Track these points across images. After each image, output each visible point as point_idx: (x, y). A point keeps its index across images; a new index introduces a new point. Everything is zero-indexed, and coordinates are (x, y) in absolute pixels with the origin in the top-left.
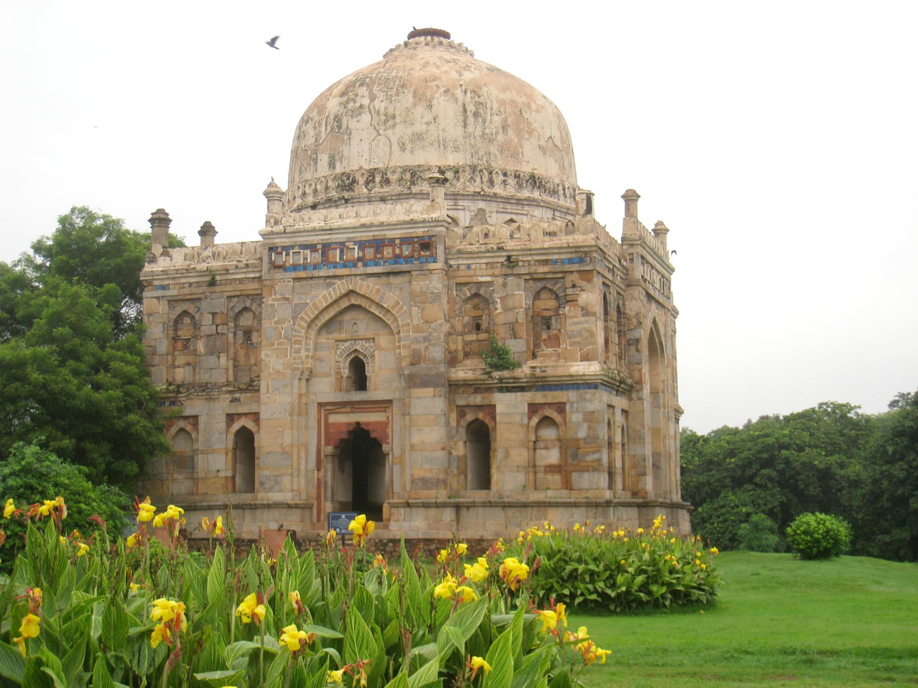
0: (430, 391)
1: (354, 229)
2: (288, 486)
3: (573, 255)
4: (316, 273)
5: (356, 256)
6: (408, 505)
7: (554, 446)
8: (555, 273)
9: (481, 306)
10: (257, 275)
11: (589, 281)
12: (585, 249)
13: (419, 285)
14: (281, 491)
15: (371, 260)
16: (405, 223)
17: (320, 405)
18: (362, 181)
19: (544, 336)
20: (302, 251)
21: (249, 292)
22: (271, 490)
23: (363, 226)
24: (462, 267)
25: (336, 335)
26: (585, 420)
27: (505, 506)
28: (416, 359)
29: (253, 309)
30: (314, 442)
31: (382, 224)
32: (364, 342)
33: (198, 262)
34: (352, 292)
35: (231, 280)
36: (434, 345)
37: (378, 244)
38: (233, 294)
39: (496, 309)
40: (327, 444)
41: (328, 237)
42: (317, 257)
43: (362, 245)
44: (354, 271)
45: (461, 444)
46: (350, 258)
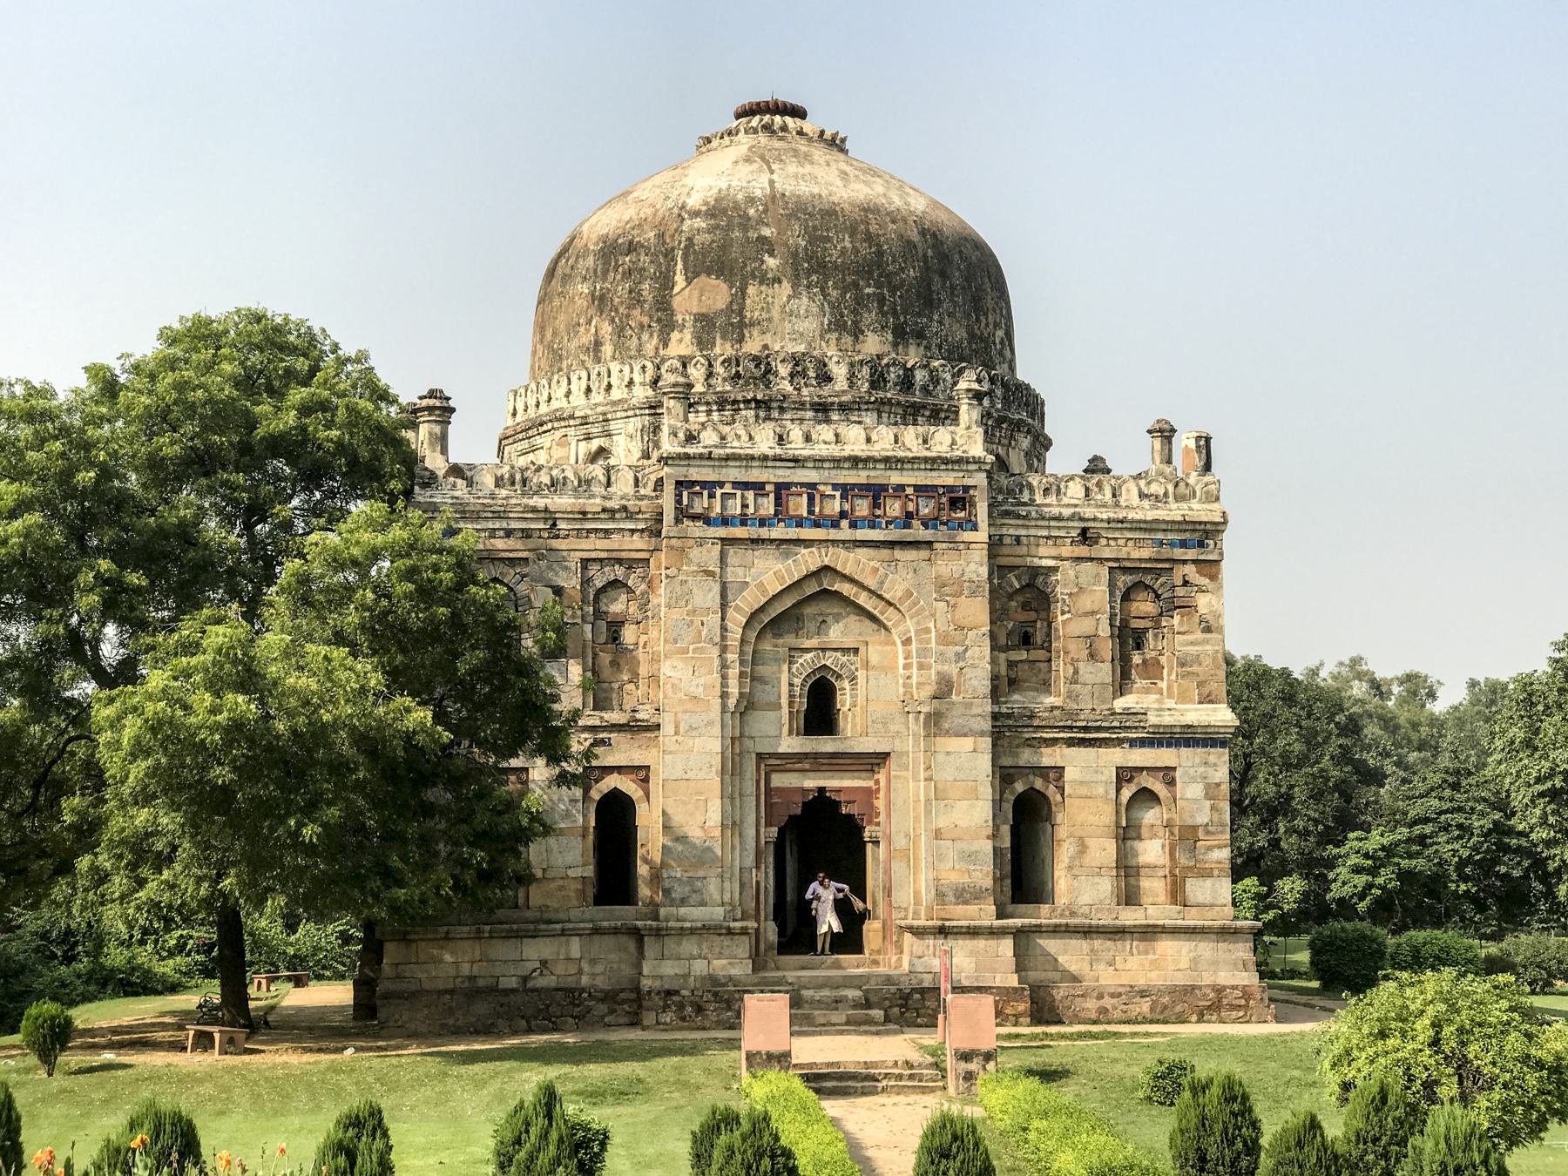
0: (967, 743)
1: (837, 462)
2: (717, 897)
3: (1187, 536)
4: (764, 533)
5: (837, 509)
6: (943, 932)
7: (1154, 836)
8: (1157, 560)
9: (1034, 604)
10: (641, 526)
11: (1214, 577)
12: (1209, 527)
13: (947, 565)
14: (703, 904)
15: (864, 518)
16: (926, 460)
17: (760, 756)
18: (784, 370)
19: (1137, 659)
20: (739, 493)
21: (624, 555)
22: (683, 902)
23: (855, 462)
24: (1007, 540)
25: (790, 640)
26: (1208, 796)
27: (1088, 932)
28: (944, 689)
29: (630, 583)
30: (751, 819)
31: (886, 460)
32: (839, 654)
33: (524, 494)
34: (826, 568)
35: (589, 531)
36: (973, 666)
37: (877, 493)
38: (593, 555)
39: (1063, 613)
40: (768, 824)
41: (788, 472)
42: (768, 506)
43: (846, 490)
44: (833, 534)
45: (1006, 830)
46: (827, 512)
